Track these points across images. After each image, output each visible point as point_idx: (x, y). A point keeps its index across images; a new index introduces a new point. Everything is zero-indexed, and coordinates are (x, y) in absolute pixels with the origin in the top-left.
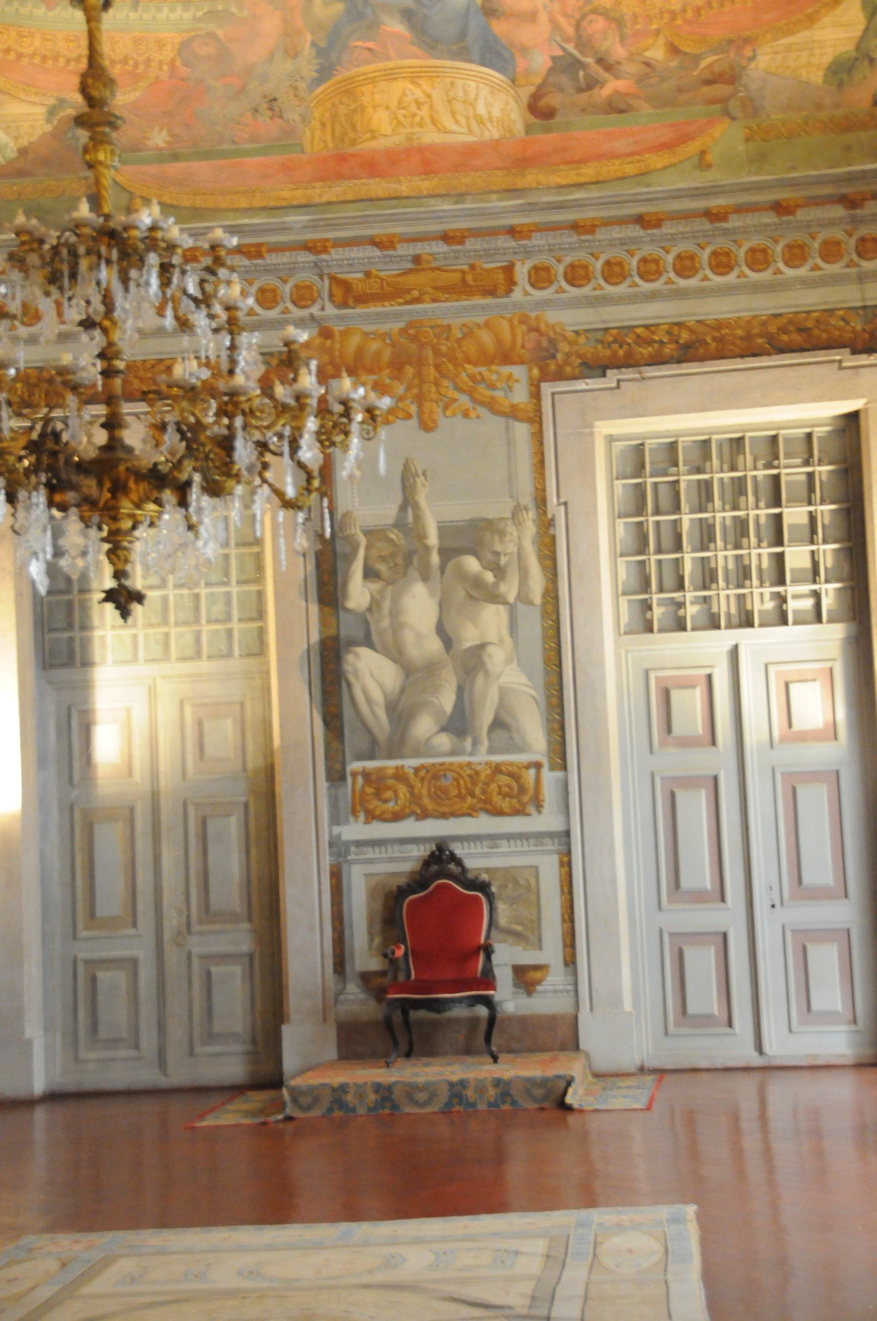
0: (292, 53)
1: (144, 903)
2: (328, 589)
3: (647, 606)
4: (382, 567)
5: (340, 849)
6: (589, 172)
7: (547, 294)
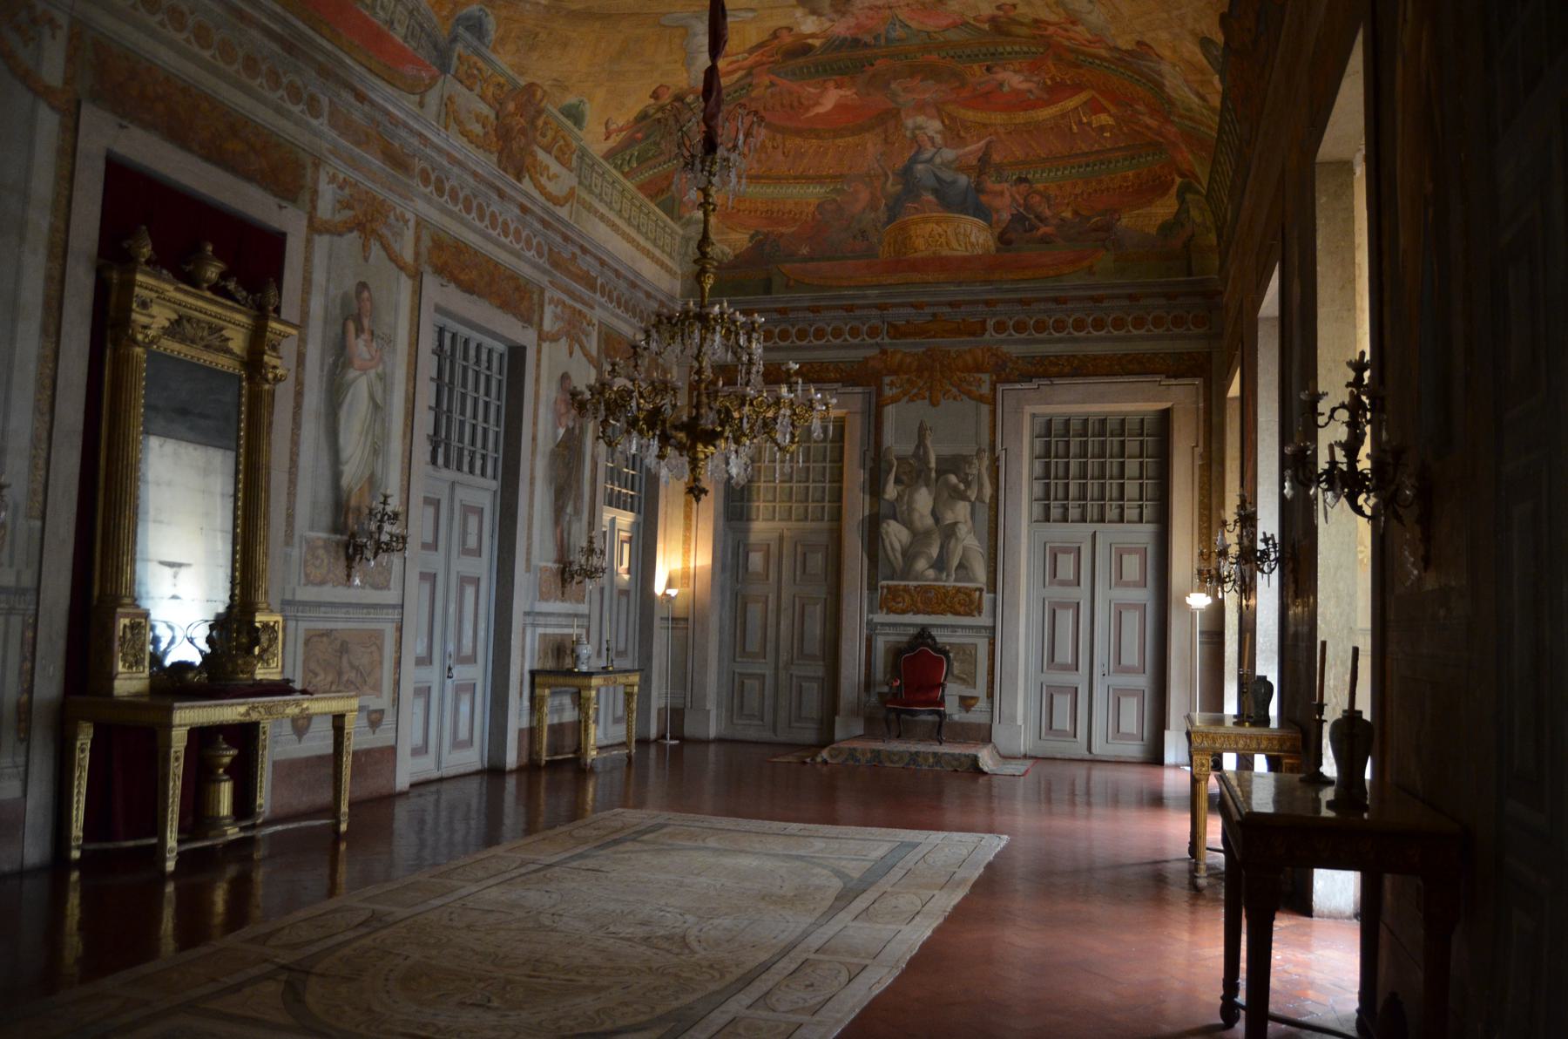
0: (875, 208)
1: (770, 646)
2: (875, 487)
3: (1047, 508)
4: (905, 478)
5: (872, 626)
7: (1003, 336)
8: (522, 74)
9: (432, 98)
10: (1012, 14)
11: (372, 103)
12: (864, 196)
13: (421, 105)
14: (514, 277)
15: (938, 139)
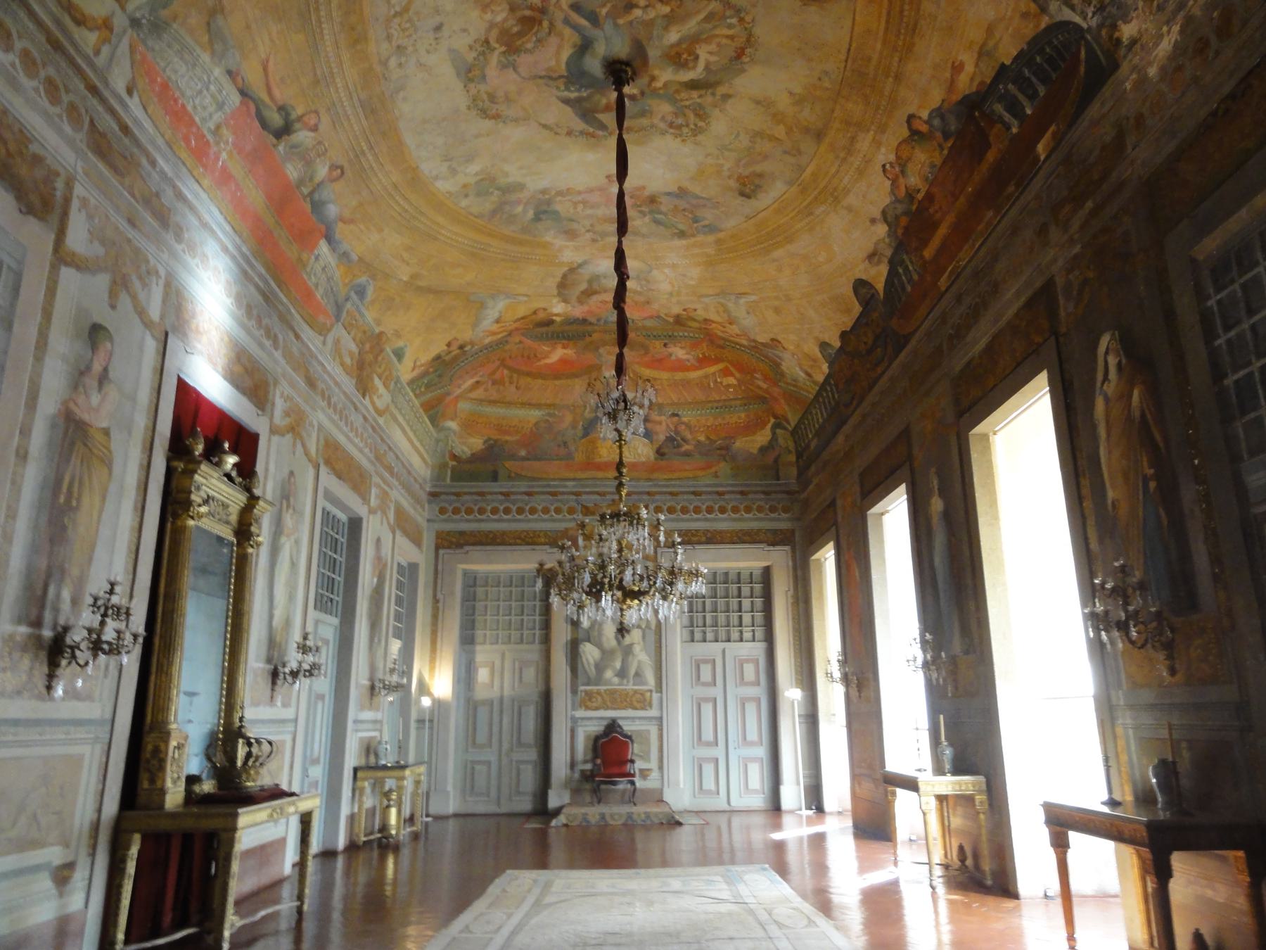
3: (692, 633)
6: (676, 475)
8: (378, 325)
9: (330, 340)
10: (692, 314)
11: (302, 342)
12: (569, 418)
13: (324, 343)
14: (360, 467)
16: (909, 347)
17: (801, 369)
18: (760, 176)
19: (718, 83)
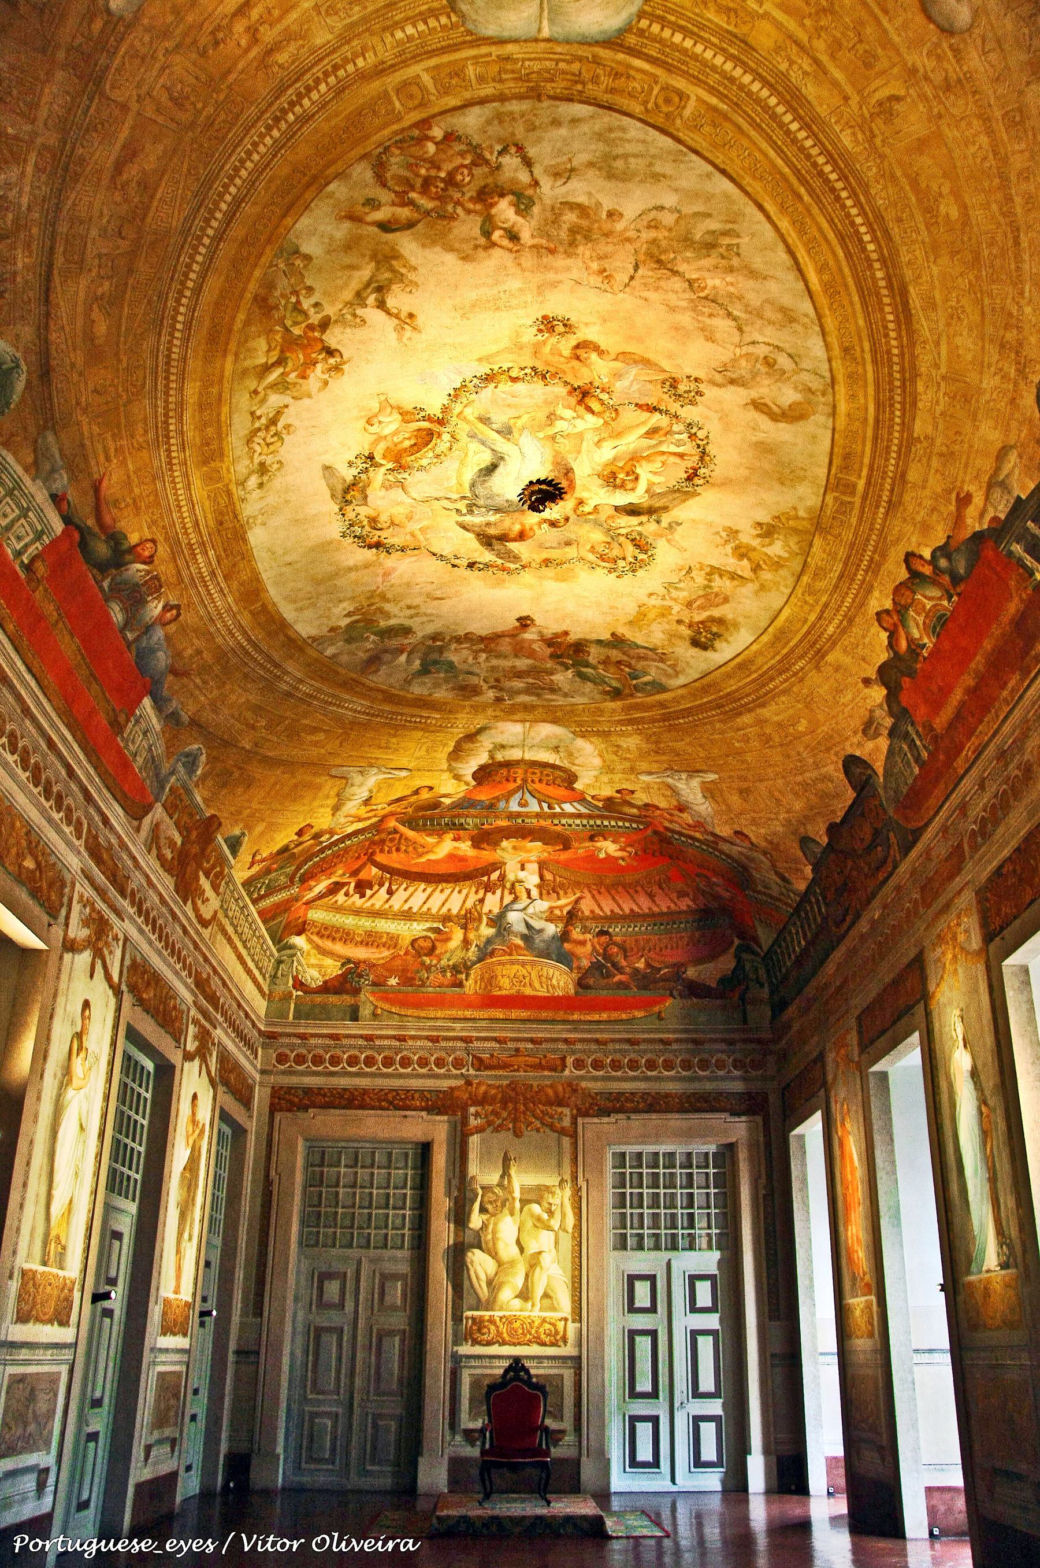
3: (624, 1237)
4: (490, 1207)
15: (535, 893)
16: (919, 847)
17: (777, 873)
18: (721, 621)
19: (666, 509)
